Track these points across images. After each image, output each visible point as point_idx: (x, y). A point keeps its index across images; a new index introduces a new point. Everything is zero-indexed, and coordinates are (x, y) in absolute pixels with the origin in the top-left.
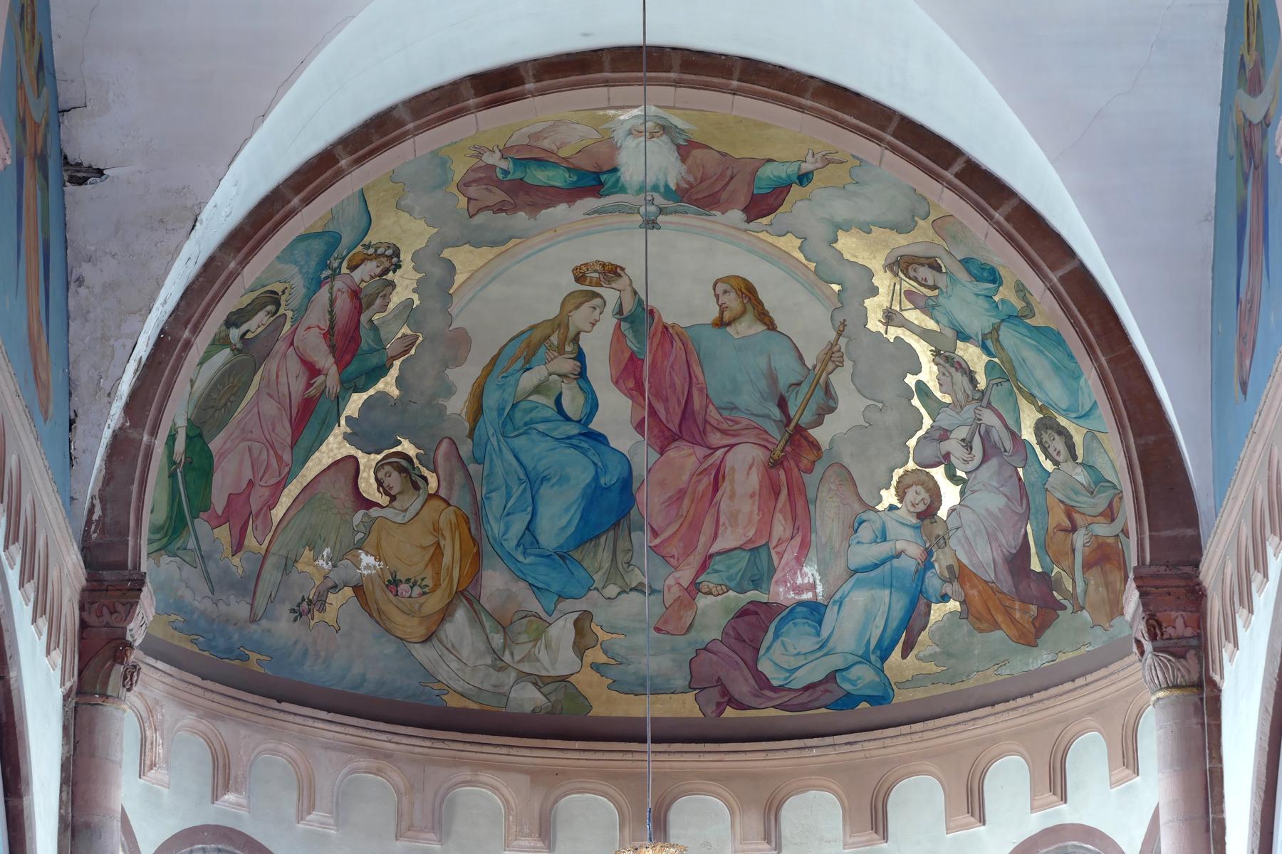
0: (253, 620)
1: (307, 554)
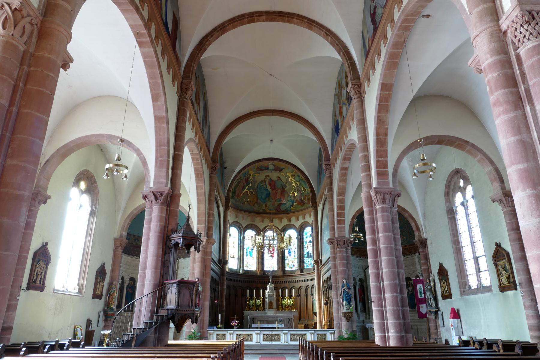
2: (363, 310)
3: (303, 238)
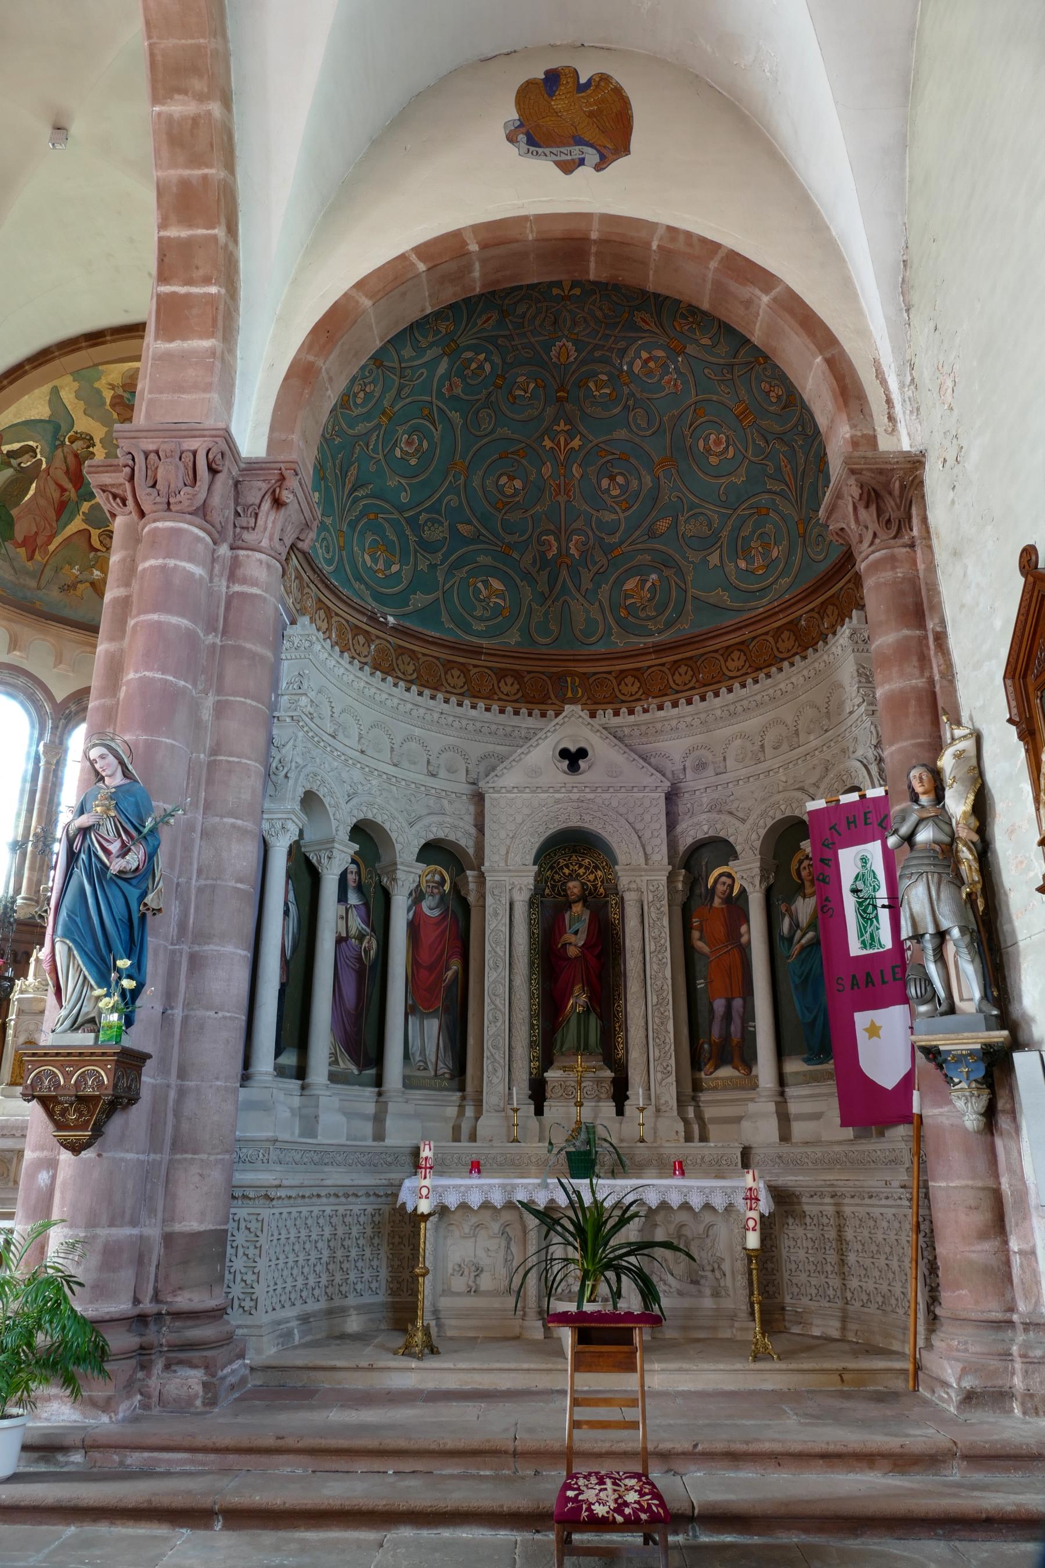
0: (39, 588)
1: (67, 567)
2: (443, 1070)
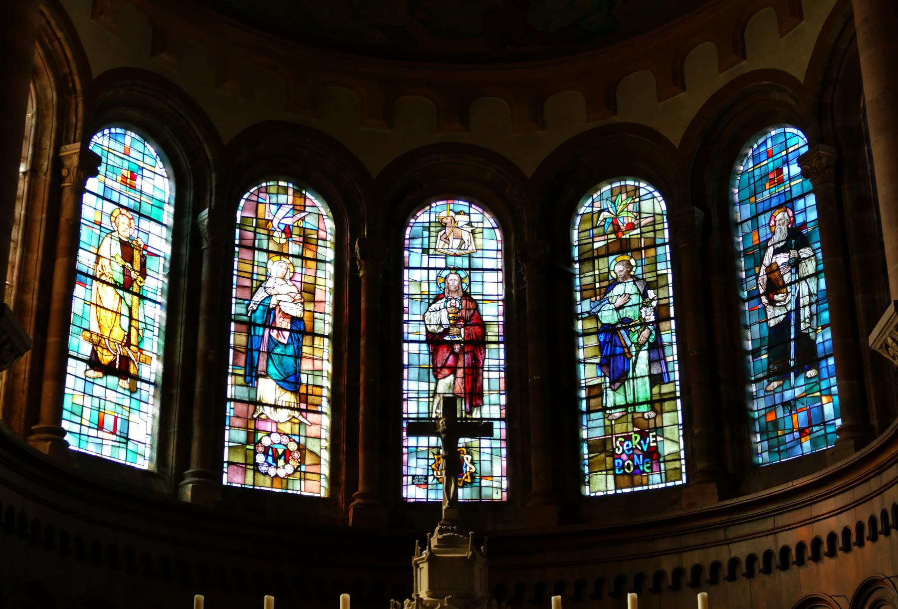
3: (729, 226)
